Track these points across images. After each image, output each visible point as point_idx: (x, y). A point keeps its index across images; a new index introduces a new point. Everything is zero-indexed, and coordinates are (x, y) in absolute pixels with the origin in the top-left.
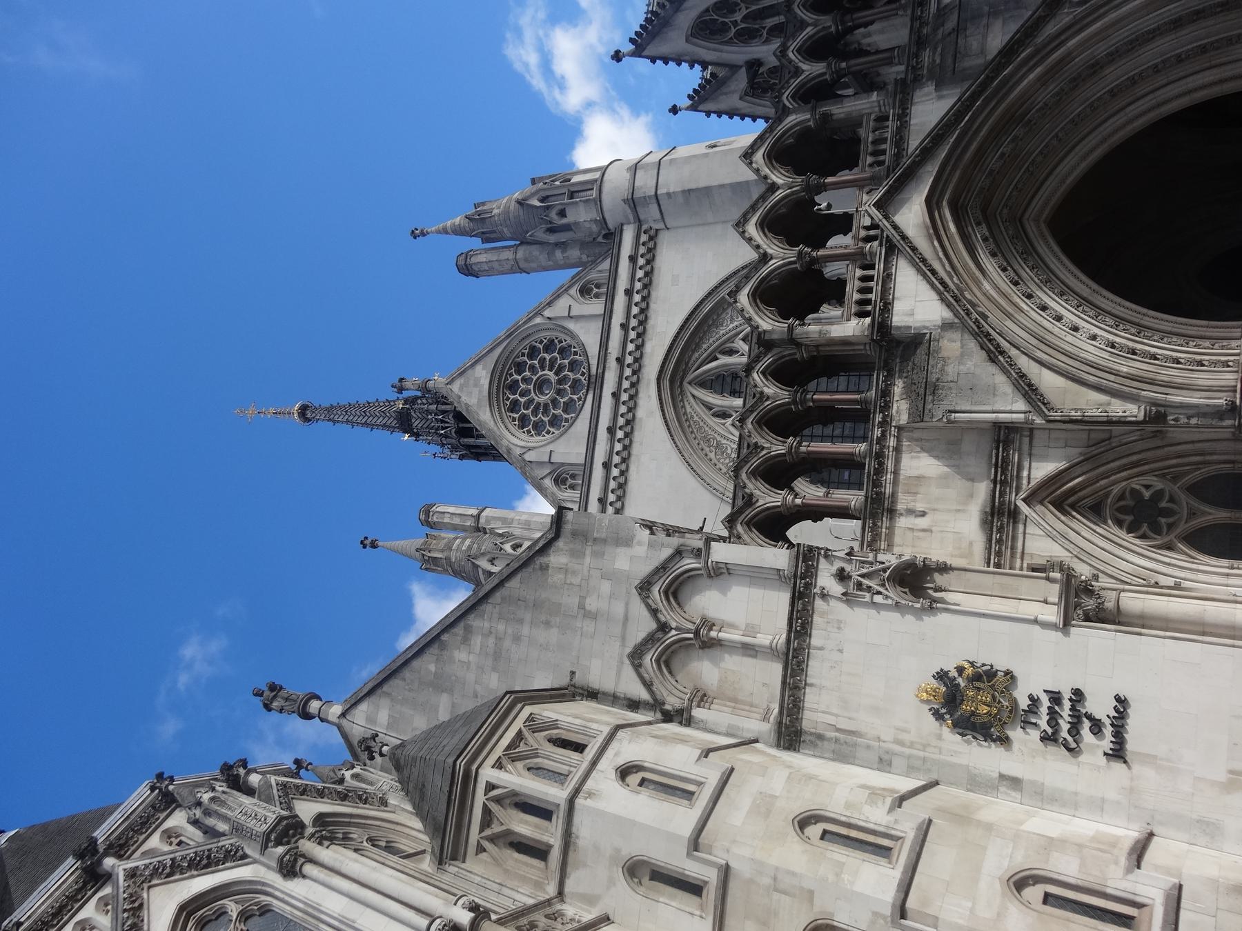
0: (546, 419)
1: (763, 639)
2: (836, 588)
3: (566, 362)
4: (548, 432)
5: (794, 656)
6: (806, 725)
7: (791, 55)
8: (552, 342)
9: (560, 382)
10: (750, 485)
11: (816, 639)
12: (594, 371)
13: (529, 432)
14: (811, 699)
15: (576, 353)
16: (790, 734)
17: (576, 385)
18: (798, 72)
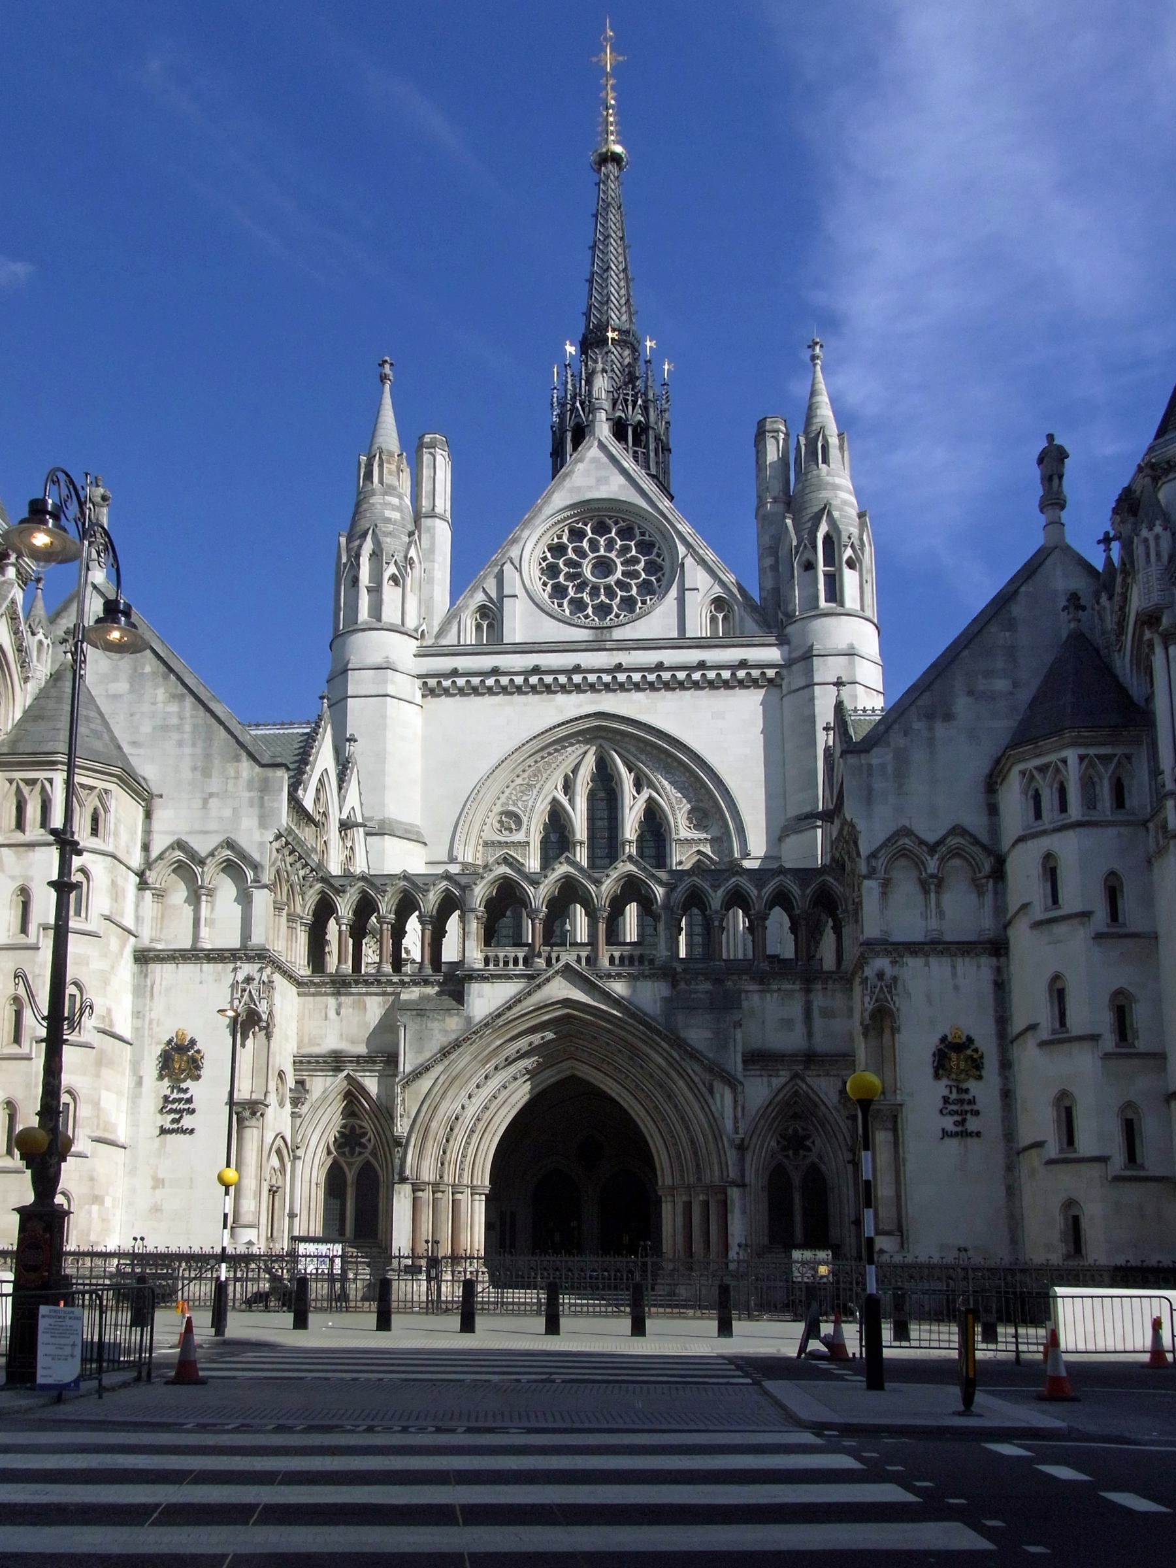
0: (561, 578)
1: (204, 932)
2: (240, 977)
3: (634, 591)
4: (545, 584)
5: (194, 955)
6: (151, 966)
7: (734, 879)
8: (661, 568)
9: (608, 588)
10: (353, 890)
11: (208, 967)
12: (618, 634)
13: (545, 559)
14: (169, 967)
15: (644, 602)
16: (143, 957)
17: (603, 610)
18: (715, 887)
